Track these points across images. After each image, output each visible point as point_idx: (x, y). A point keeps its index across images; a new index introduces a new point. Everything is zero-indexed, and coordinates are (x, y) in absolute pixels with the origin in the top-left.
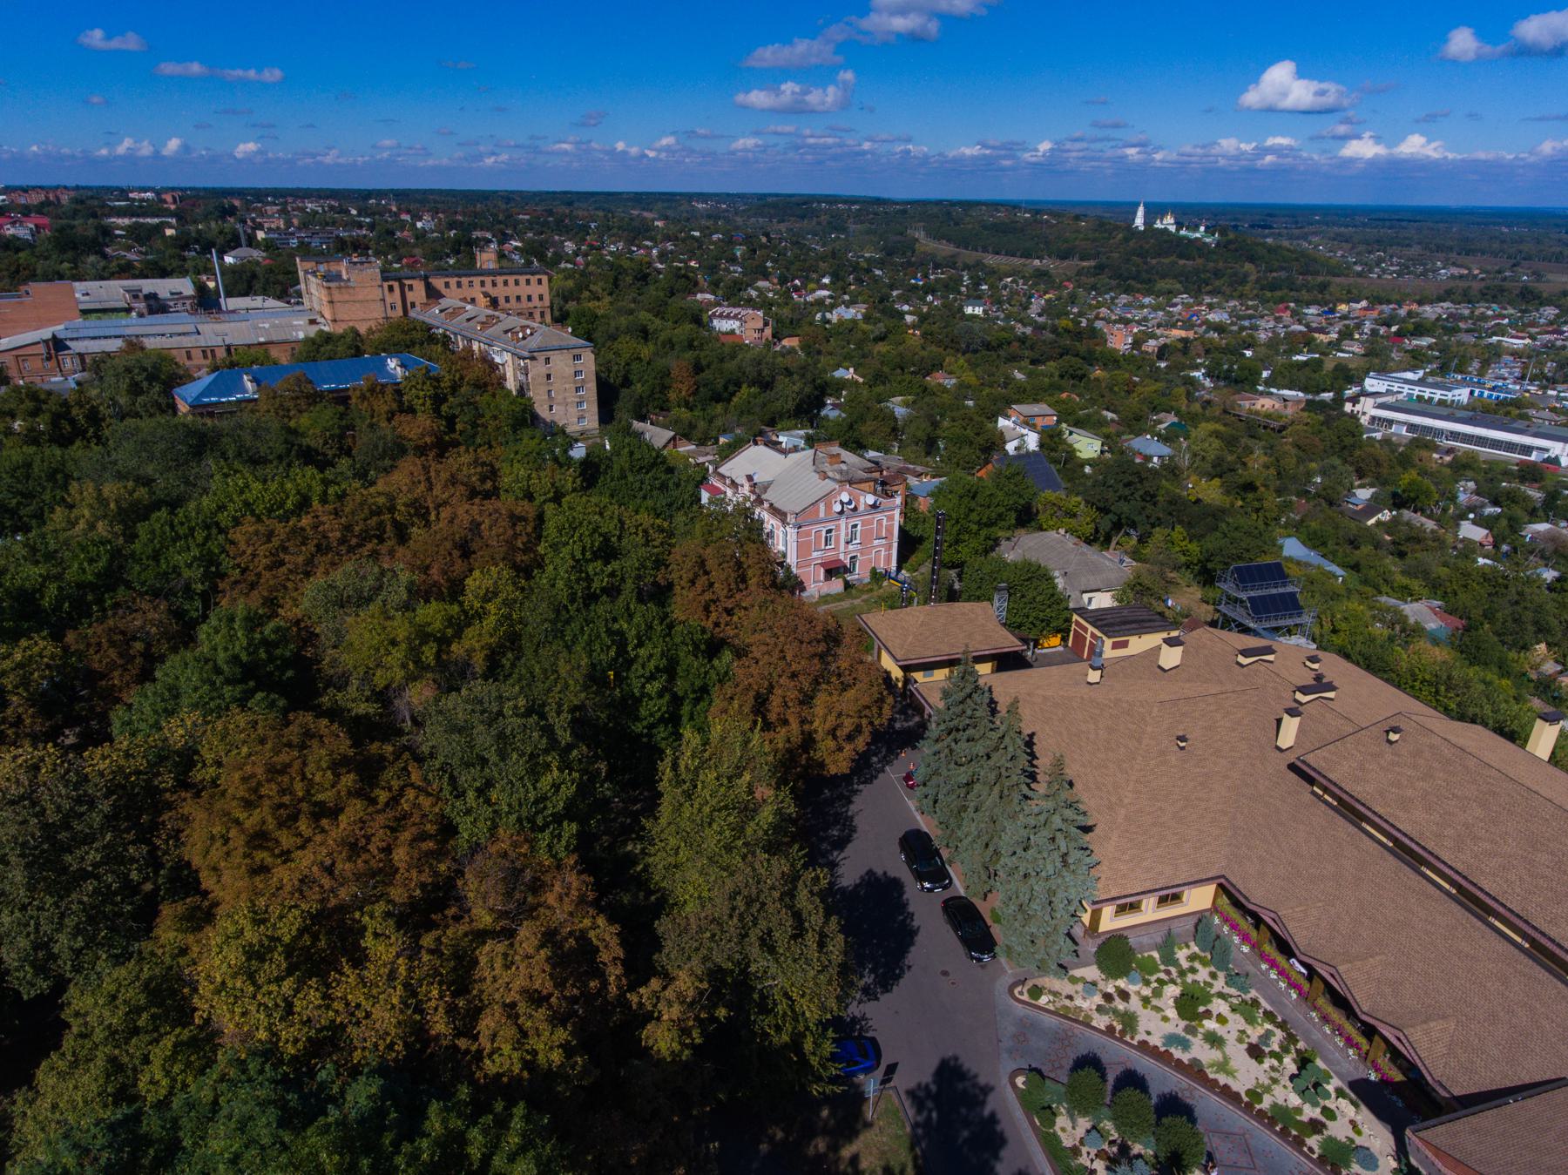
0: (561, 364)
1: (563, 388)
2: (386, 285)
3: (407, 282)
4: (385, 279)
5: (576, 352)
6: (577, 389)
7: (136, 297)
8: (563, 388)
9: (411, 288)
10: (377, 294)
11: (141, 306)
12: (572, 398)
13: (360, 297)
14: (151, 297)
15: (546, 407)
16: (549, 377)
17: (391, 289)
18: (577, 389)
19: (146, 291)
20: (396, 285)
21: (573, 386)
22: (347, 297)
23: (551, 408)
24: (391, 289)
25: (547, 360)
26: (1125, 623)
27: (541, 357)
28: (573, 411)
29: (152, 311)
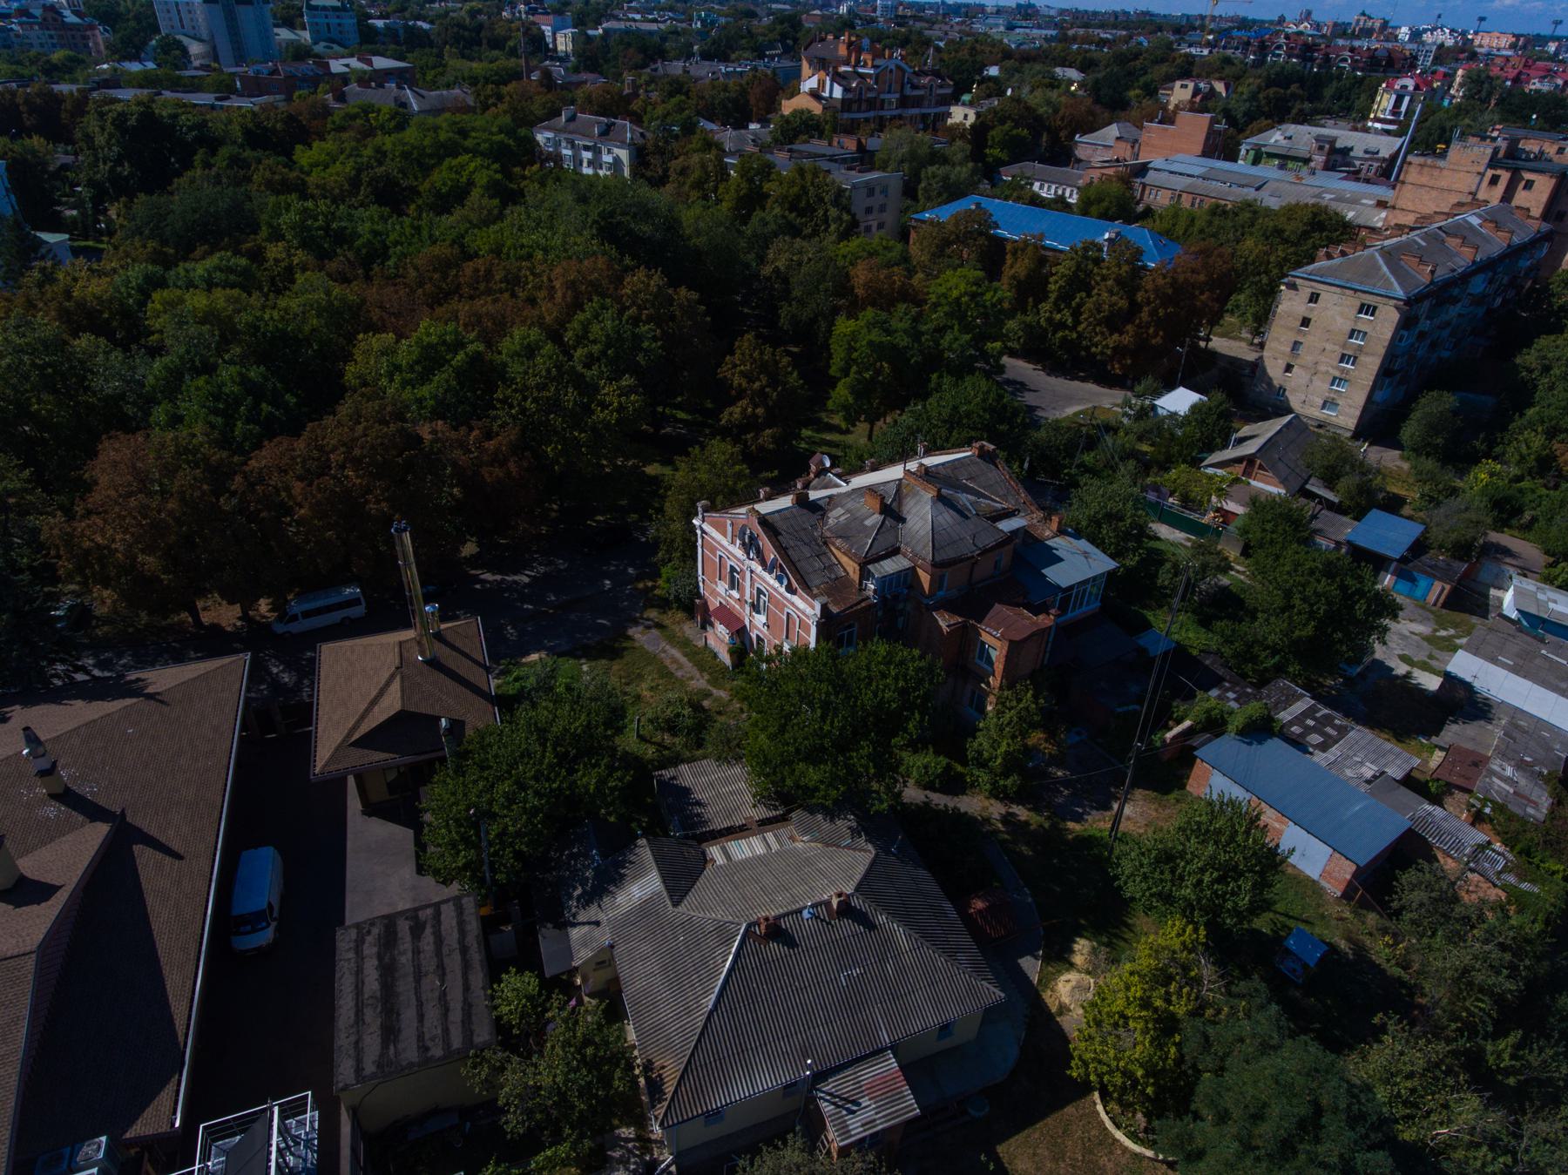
0: (1336, 310)
1: (1321, 348)
2: (1490, 173)
3: (1527, 176)
4: (1494, 163)
5: (1369, 300)
6: (1343, 358)
7: (1321, 148)
8: (1321, 348)
9: (1529, 185)
10: (1470, 182)
11: (1319, 159)
12: (1329, 366)
13: (1443, 184)
14: (1346, 151)
15: (1282, 364)
16: (1306, 322)
17: (1494, 181)
18: (1343, 358)
19: (1339, 145)
20: (1505, 176)
21: (1339, 351)
22: (1424, 180)
23: (1289, 368)
24: (1494, 181)
25: (1314, 298)
26: (388, 971)
27: (1306, 290)
28: (1321, 388)
29: (1329, 167)
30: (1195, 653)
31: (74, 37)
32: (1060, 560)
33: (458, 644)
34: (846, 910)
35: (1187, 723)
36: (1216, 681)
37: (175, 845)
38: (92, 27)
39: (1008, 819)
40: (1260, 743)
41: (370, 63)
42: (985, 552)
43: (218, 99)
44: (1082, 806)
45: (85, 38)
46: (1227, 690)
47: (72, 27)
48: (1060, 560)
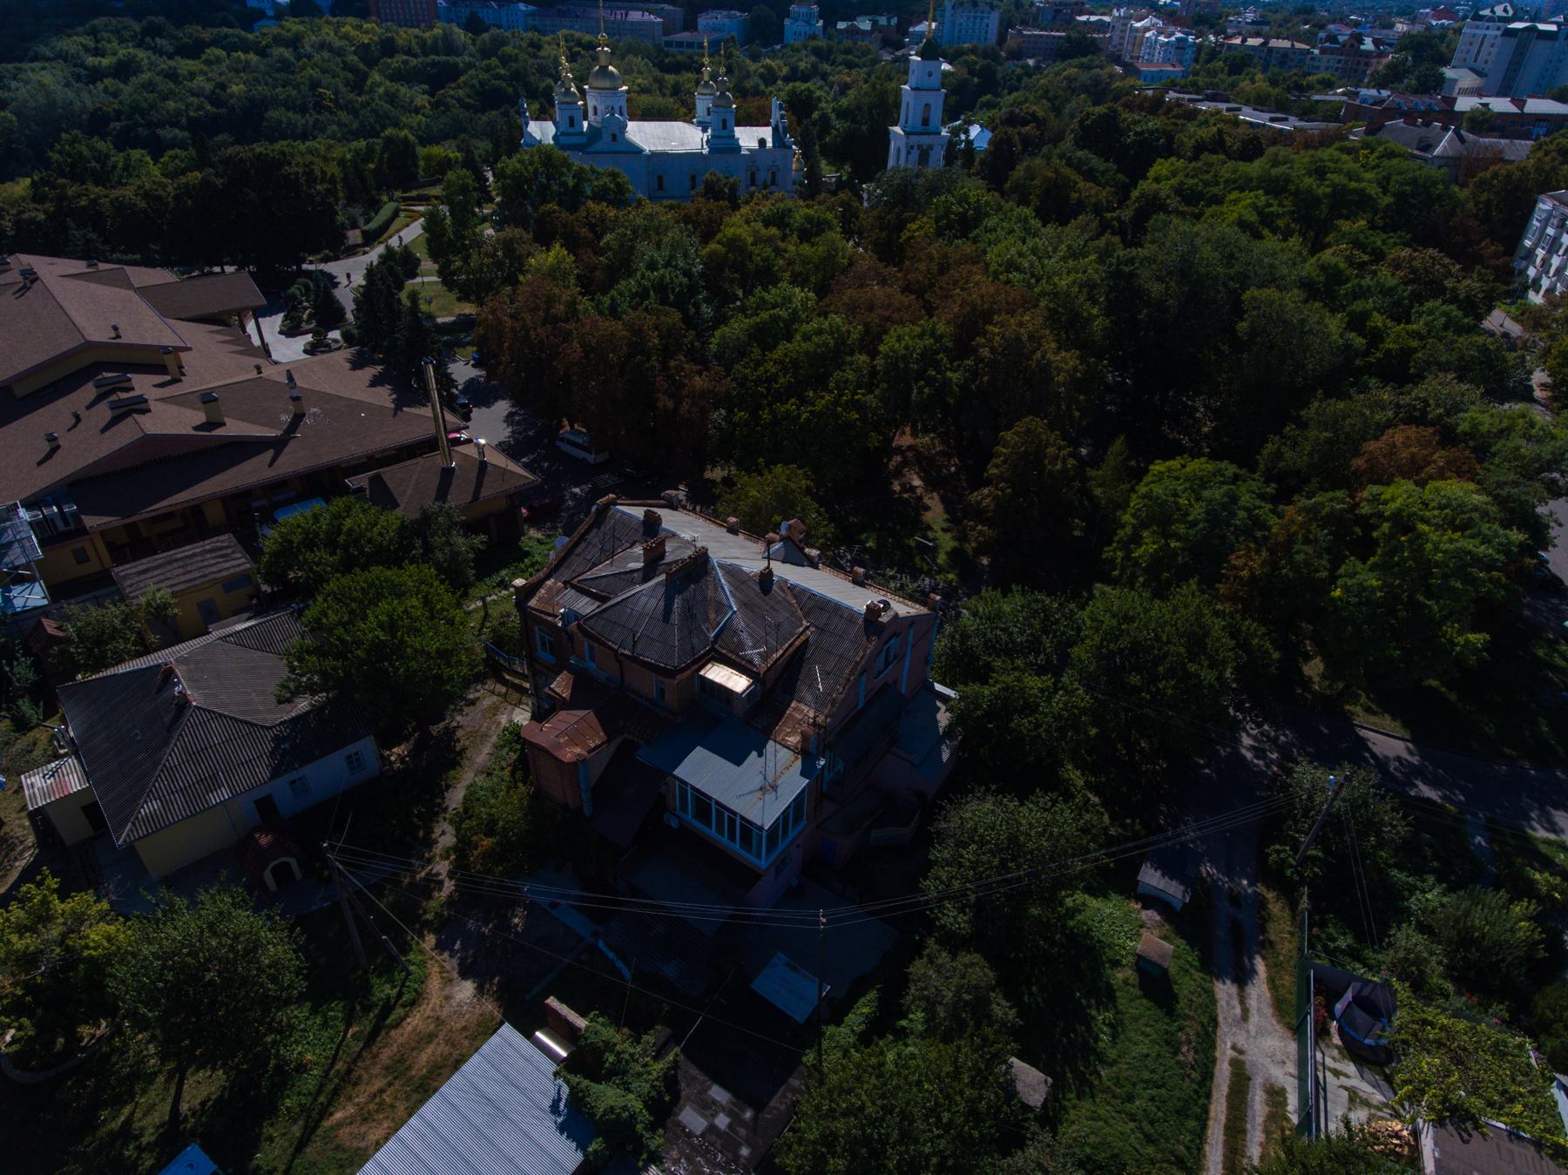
30: (809, 1058)
31: (1353, 64)
33: (487, 480)
34: (183, 704)
35: (581, 1023)
36: (750, 1094)
37: (280, 460)
38: (1381, 55)
39: (434, 882)
40: (562, 1128)
41: (1520, 103)
42: (634, 659)
43: (1272, 120)
44: (464, 948)
45: (1367, 64)
46: (730, 1114)
47: (1367, 54)
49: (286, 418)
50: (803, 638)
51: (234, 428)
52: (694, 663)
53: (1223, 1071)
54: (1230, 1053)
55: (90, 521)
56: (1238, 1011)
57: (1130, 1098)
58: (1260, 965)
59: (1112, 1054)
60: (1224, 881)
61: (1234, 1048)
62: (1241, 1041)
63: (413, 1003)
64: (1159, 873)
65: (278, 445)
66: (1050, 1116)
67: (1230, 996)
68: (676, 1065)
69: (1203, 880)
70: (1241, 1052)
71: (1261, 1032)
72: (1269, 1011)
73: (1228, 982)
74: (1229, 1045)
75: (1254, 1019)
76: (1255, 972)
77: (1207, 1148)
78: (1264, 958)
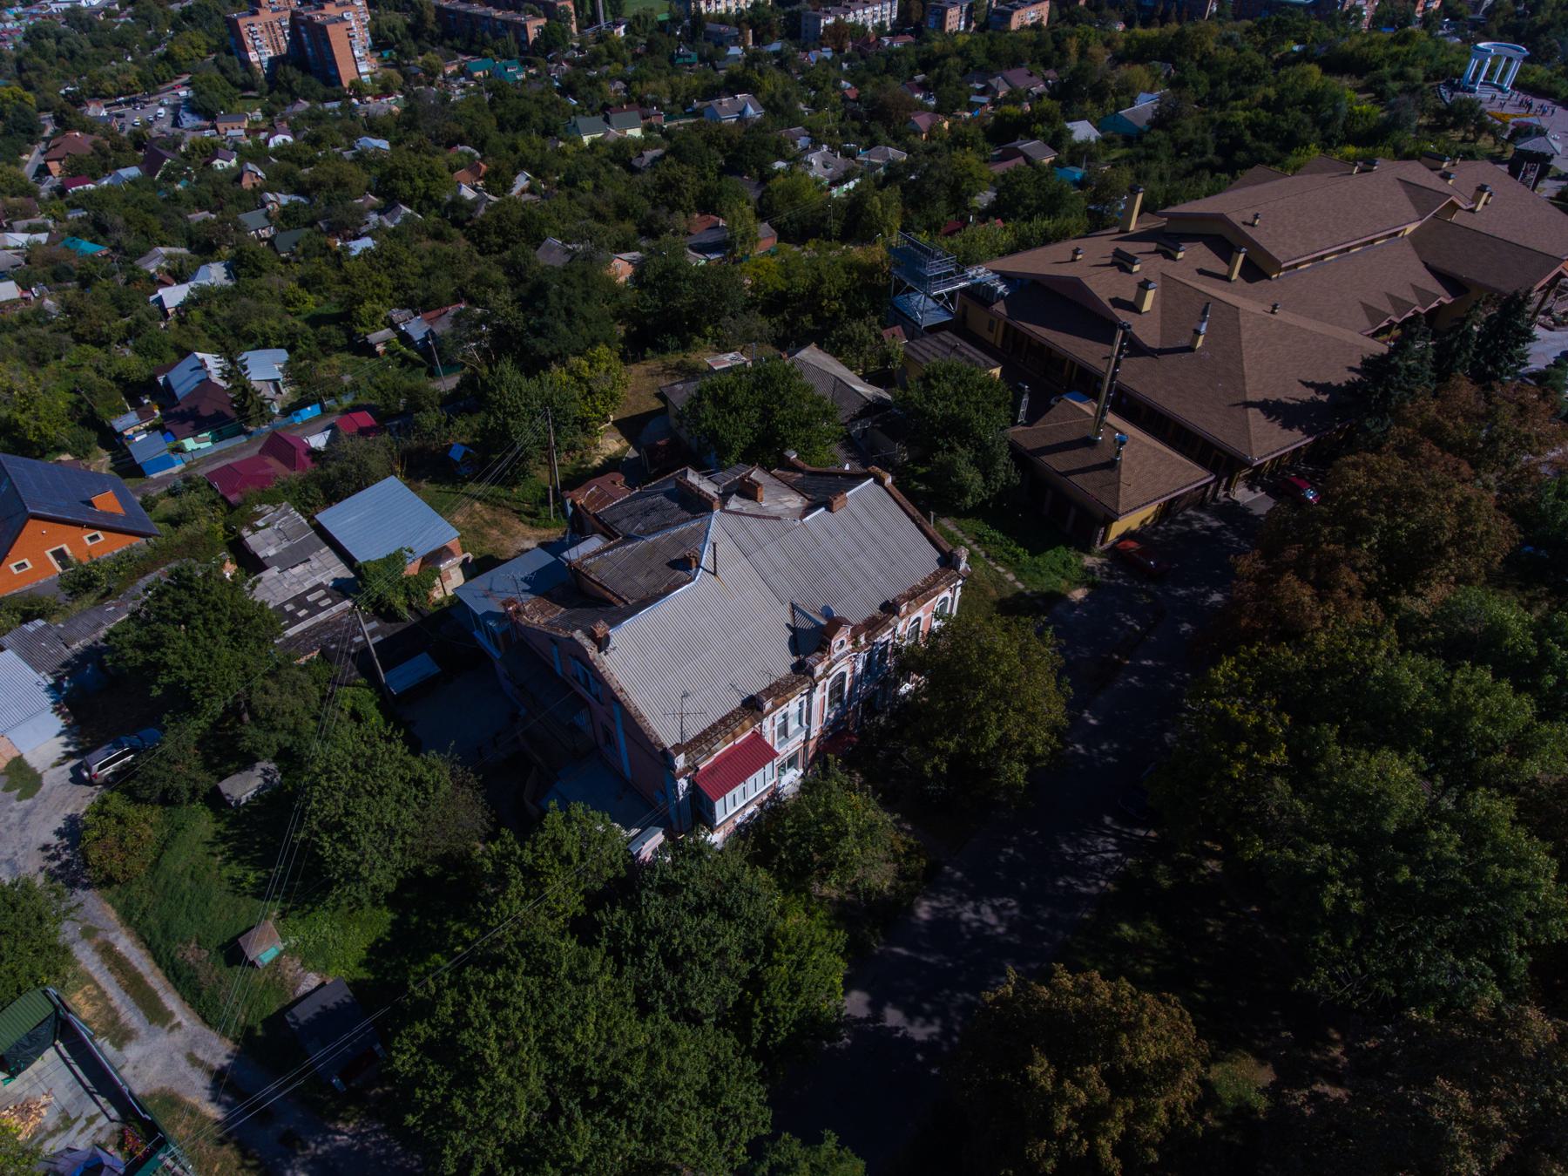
32: (525, 580)
33: (1097, 474)
48: (525, 580)
49: (1185, 342)
50: (614, 599)
51: (1147, 325)
52: (606, 526)
53: (171, 1001)
54: (179, 1018)
55: (1000, 307)
56: (199, 1054)
57: (192, 877)
58: (214, 1112)
59: (225, 872)
60: (317, 1148)
61: (179, 1025)
62: (178, 1037)
63: (532, 524)
64: (331, 1005)
65: (1135, 348)
66: (216, 801)
67: (215, 1055)
68: (401, 620)
69: (335, 1119)
70: (172, 1029)
71: (170, 1063)
72: (178, 1087)
73: (226, 1062)
74: (185, 1023)
75: (183, 1066)
76: (214, 1099)
77: (143, 952)
78: (218, 1122)
